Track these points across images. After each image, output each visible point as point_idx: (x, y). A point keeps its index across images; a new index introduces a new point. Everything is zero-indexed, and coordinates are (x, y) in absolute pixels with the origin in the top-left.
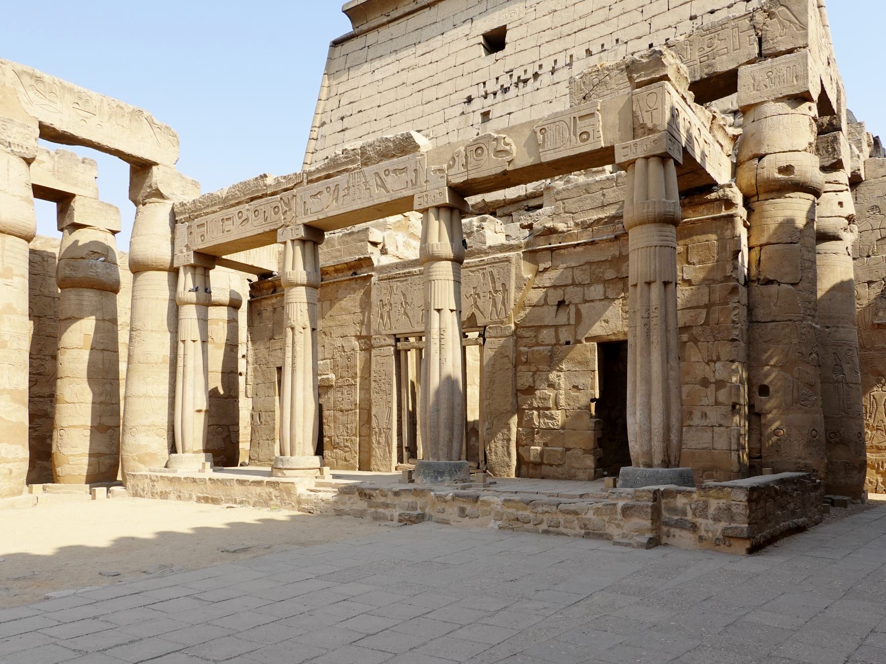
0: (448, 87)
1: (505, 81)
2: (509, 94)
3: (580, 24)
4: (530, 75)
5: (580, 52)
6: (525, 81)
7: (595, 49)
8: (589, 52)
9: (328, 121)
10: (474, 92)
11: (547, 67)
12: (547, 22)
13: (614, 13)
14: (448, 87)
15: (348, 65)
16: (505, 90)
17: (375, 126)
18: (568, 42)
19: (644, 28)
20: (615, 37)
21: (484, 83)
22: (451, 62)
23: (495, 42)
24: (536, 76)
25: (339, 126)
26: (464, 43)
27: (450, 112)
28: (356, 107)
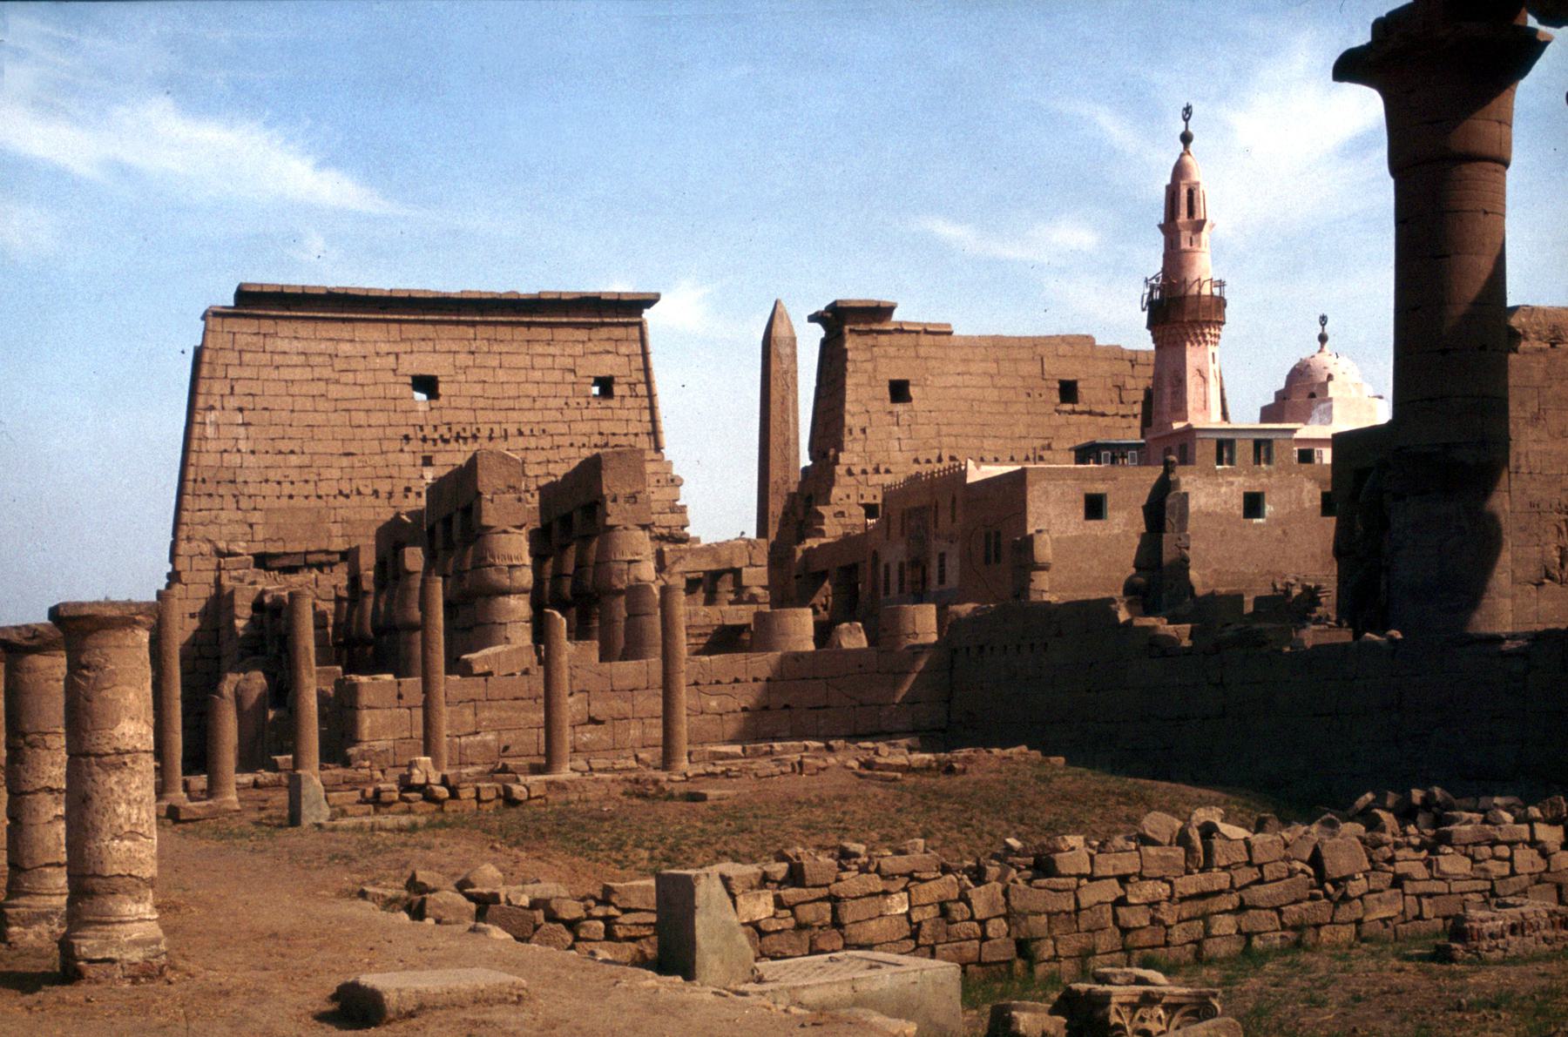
0: (381, 418)
1: (443, 430)
2: (448, 447)
3: (511, 404)
4: (468, 434)
5: (512, 430)
6: (465, 439)
7: (526, 430)
8: (521, 433)
9: (218, 405)
10: (410, 432)
11: (485, 432)
12: (477, 389)
13: (538, 404)
14: (381, 418)
15: (237, 347)
16: (446, 441)
17: (290, 432)
18: (501, 416)
19: (563, 428)
20: (542, 426)
21: (421, 428)
22: (380, 391)
23: (427, 384)
24: (475, 437)
25: (239, 418)
26: (390, 377)
27: (386, 446)
28: (261, 402)
